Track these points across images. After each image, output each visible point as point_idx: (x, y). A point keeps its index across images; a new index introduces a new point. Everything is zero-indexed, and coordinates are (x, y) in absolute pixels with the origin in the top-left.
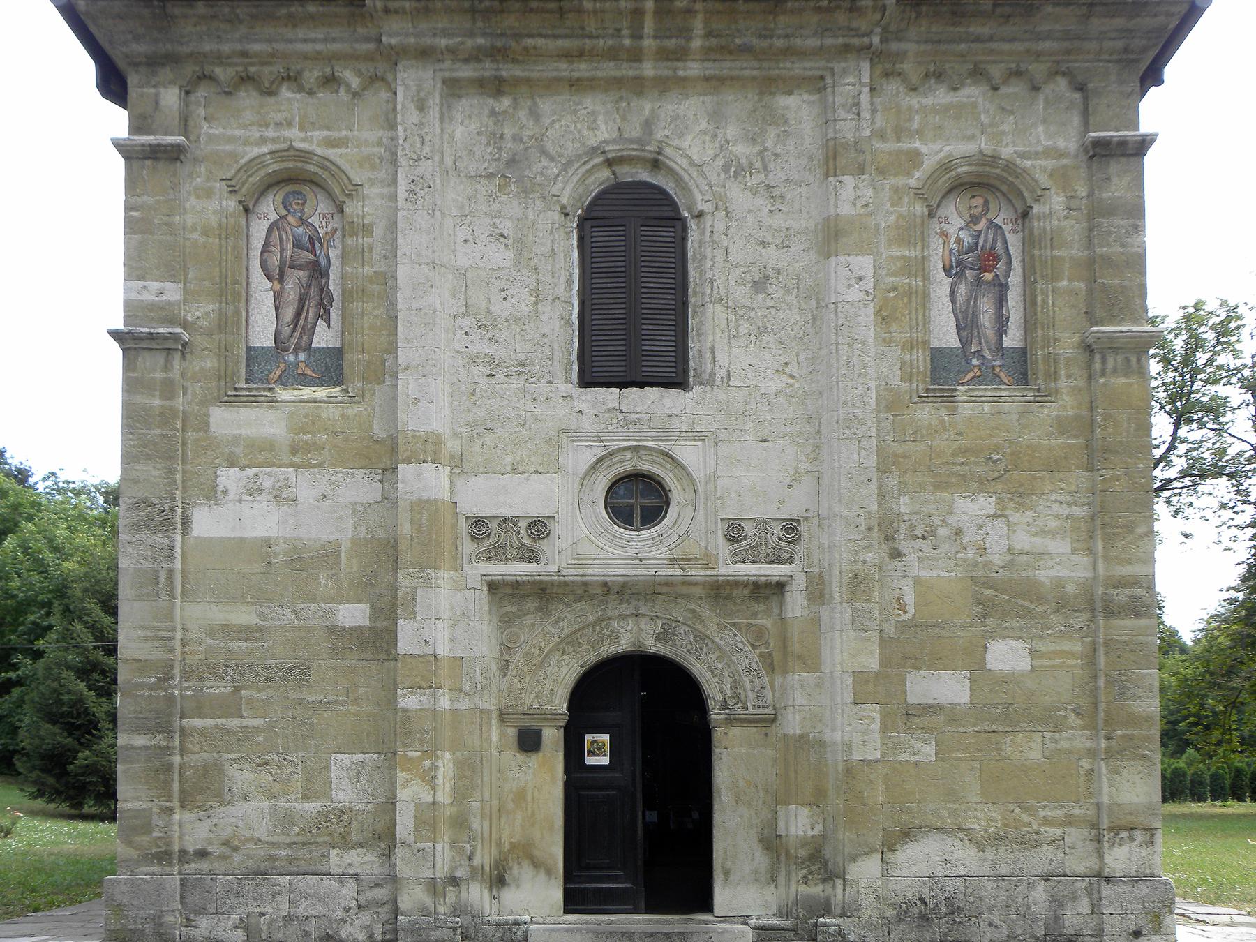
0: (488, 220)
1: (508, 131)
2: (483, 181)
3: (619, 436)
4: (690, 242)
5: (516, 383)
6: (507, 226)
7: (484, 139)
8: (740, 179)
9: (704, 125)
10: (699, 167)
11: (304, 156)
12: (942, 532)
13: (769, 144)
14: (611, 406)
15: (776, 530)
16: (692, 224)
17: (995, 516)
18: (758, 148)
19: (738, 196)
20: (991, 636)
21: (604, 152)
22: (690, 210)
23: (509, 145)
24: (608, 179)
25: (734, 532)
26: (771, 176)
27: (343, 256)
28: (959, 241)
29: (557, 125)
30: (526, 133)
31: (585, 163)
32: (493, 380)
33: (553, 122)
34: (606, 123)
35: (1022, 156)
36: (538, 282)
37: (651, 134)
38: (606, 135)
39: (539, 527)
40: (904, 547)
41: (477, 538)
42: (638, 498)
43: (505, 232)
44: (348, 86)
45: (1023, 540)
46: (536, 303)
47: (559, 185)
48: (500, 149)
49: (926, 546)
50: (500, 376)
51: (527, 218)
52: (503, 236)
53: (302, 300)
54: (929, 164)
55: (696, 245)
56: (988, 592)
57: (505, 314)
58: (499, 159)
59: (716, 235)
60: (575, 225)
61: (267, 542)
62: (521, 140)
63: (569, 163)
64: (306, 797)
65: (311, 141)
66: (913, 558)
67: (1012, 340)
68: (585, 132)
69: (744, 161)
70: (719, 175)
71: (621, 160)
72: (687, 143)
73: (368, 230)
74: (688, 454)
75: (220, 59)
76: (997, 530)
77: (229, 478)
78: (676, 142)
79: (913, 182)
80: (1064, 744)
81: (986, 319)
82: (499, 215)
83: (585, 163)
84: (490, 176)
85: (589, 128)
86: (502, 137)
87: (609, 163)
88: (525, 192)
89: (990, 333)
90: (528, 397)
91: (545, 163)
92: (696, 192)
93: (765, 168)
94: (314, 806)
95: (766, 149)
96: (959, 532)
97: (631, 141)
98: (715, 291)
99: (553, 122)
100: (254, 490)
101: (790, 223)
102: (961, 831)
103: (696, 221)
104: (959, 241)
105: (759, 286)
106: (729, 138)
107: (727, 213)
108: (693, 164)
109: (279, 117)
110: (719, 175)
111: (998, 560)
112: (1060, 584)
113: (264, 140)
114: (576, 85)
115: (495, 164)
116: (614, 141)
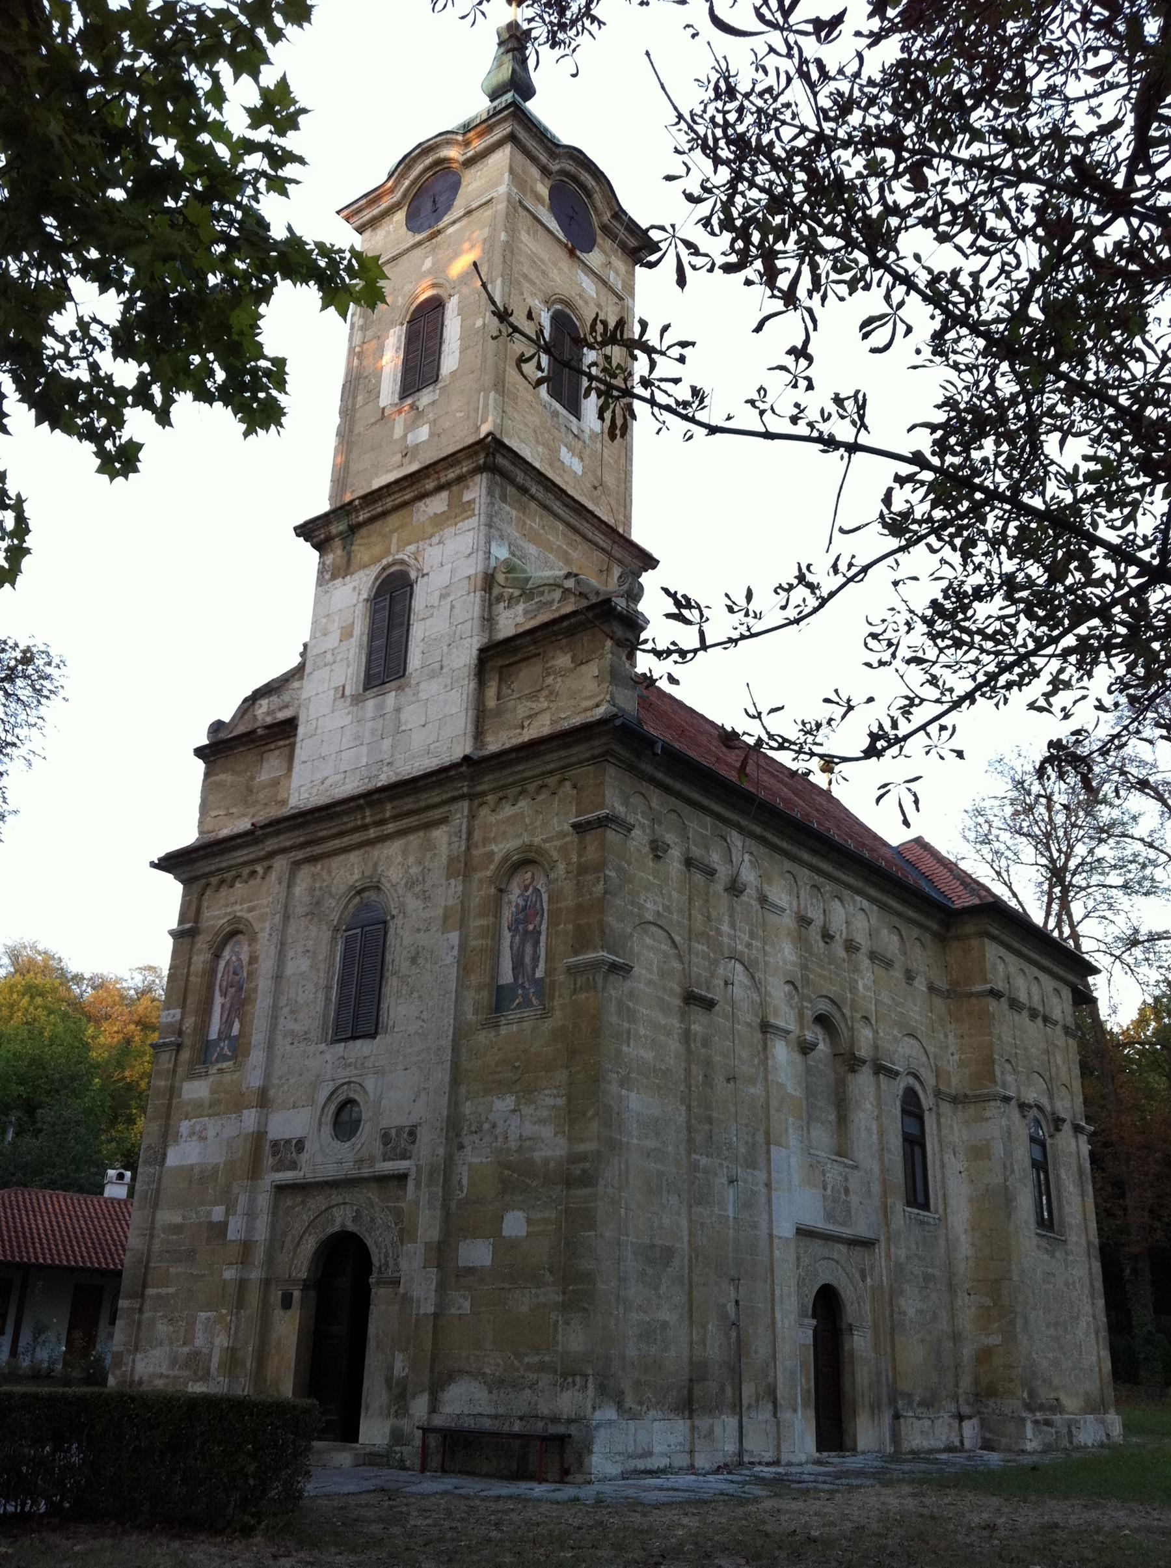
3: (343, 1075)
12: (486, 1126)
17: (514, 1111)
20: (506, 1208)
25: (386, 1138)
28: (517, 905)
35: (544, 841)
39: (300, 1145)
40: (466, 1140)
41: (274, 1154)
45: (529, 1129)
49: (476, 1138)
54: (498, 858)
56: (507, 1172)
61: (192, 1167)
66: (469, 1149)
67: (539, 973)
74: (370, 1084)
75: (211, 874)
76: (515, 1120)
79: (489, 873)
80: (542, 1299)
81: (527, 960)
89: (529, 969)
94: (186, 1350)
96: (494, 1126)
100: (192, 1134)
102: (478, 1375)
104: (517, 905)
105: (414, 960)
111: (513, 1145)
112: (546, 1161)
114: (346, 850)
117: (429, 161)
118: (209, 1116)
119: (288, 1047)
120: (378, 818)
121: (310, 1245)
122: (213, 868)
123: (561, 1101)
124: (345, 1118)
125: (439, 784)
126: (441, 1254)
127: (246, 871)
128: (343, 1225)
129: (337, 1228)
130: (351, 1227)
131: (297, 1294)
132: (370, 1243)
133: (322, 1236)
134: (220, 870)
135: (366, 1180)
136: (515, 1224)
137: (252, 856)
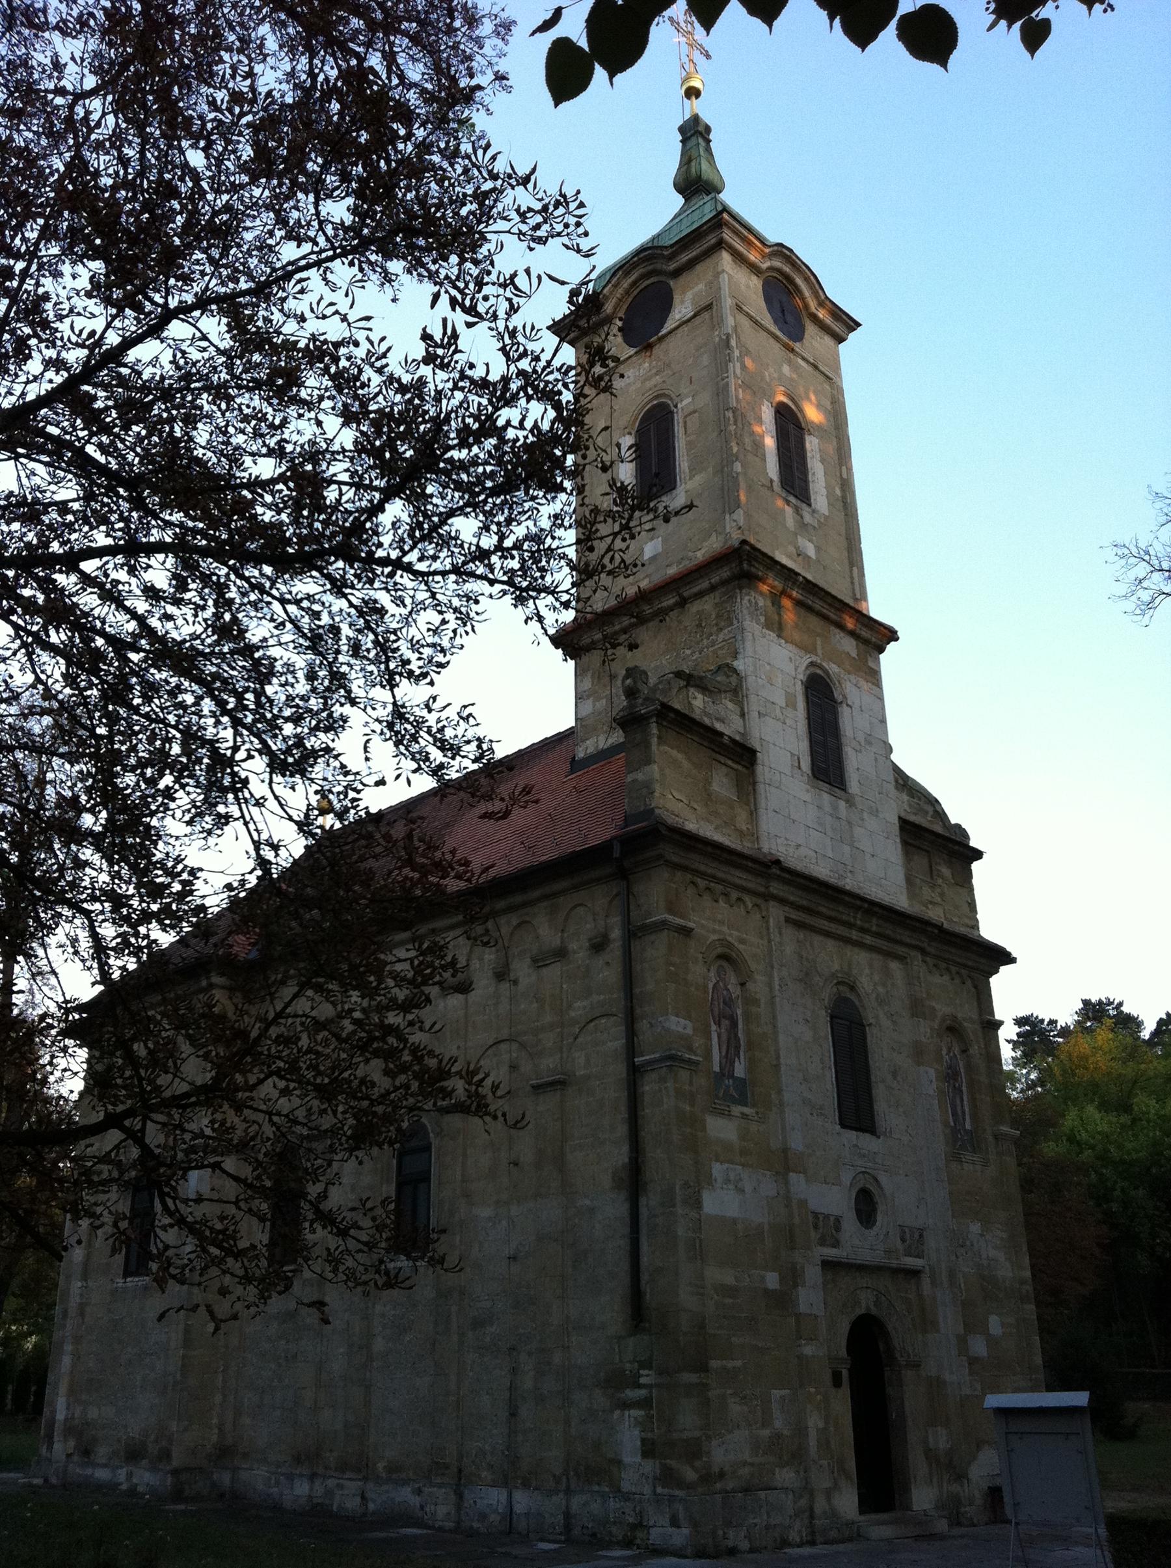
11: (730, 945)
15: (916, 1236)
19: (886, 1023)
27: (747, 1016)
41: (816, 1227)
42: (866, 1205)
44: (746, 907)
45: (992, 1253)
53: (729, 1039)
61: (734, 1221)
64: (764, 1426)
65: (732, 936)
67: (968, 1126)
73: (756, 1002)
74: (883, 1179)
75: (702, 875)
77: (717, 1169)
94: (766, 1433)
100: (727, 1181)
105: (894, 1074)
109: (720, 917)
113: (714, 931)
114: (828, 934)
117: (787, 269)
118: (743, 1165)
120: (866, 925)
121: (844, 1327)
122: (710, 871)
123: (1004, 1235)
124: (866, 1205)
125: (805, 889)
126: (962, 1343)
127: (734, 895)
128: (868, 1308)
129: (863, 1311)
130: (874, 1311)
131: (845, 1373)
132: (890, 1327)
133: (853, 1317)
134: (714, 877)
135: (889, 1268)
136: (995, 1325)
137: (750, 885)
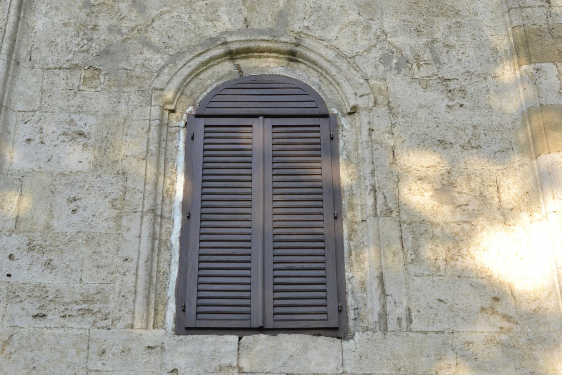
0: (64, 116)
1: (103, 22)
2: (63, 74)
4: (341, 143)
5: (79, 327)
6: (89, 123)
7: (71, 30)
8: (404, 71)
9: (354, 16)
10: (351, 60)
13: (438, 36)
14: (226, 361)
16: (344, 121)
18: (424, 40)
21: (225, 43)
22: (338, 106)
23: (102, 35)
24: (230, 73)
26: (445, 69)
29: (167, 17)
30: (125, 26)
31: (198, 55)
32: (41, 323)
33: (162, 13)
34: (229, 14)
36: (125, 190)
37: (286, 24)
38: (229, 26)
43: (86, 130)
46: (119, 217)
47: (164, 78)
48: (91, 40)
50: (54, 317)
51: (117, 114)
52: (81, 134)
55: (350, 147)
57: (72, 231)
58: (87, 51)
59: (374, 135)
60: (182, 124)
62: (119, 32)
63: (180, 54)
68: (202, 23)
69: (408, 53)
70: (376, 67)
71: (247, 52)
72: (332, 34)
78: (319, 33)
82: (80, 110)
83: (198, 55)
84: (73, 68)
85: (207, 19)
86: (95, 28)
87: (232, 55)
88: (119, 85)
90: (94, 347)
91: (148, 54)
92: (346, 86)
93: (437, 60)
95: (435, 41)
97: (261, 32)
98: (380, 201)
99: (162, 13)
101: (476, 120)
103: (349, 118)
106: (386, 29)
107: (391, 109)
108: (340, 54)
110: (376, 67)
115: (81, 55)
116: (239, 32)
119: (27, 325)
